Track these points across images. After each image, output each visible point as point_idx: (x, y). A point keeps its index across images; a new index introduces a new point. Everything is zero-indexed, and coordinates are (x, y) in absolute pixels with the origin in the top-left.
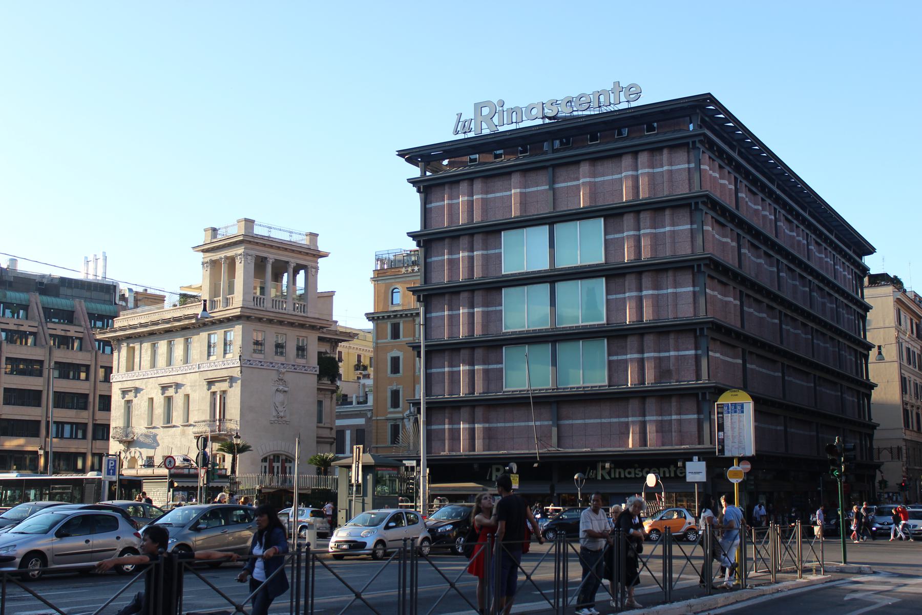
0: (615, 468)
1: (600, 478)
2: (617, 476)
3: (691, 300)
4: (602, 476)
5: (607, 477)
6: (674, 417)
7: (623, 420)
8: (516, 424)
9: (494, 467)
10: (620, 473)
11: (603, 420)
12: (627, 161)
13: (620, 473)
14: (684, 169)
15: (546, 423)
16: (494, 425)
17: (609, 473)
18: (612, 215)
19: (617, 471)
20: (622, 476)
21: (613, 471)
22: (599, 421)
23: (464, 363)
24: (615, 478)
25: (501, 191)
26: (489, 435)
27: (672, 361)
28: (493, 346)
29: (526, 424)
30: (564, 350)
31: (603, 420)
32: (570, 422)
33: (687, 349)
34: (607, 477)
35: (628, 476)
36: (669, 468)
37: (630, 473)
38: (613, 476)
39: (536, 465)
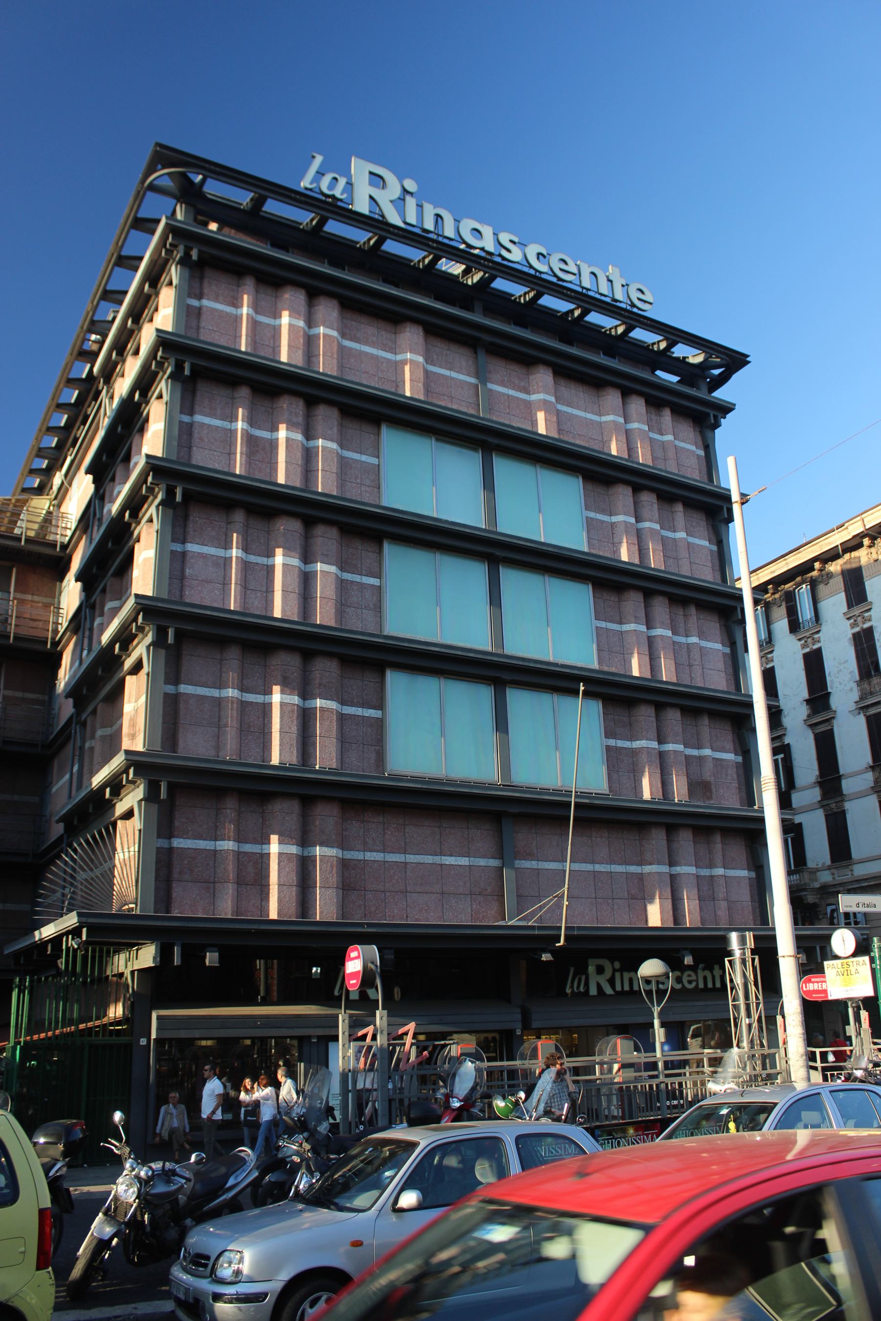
0: (622, 970)
1: (593, 991)
2: (627, 988)
3: (721, 665)
4: (599, 987)
5: (609, 991)
6: (720, 871)
7: (633, 869)
8: (411, 858)
11: (598, 868)
12: (613, 398)
14: (693, 452)
15: (482, 862)
16: (358, 855)
18: (599, 473)
21: (618, 975)
22: (589, 867)
23: (286, 686)
24: (623, 993)
25: (373, 345)
26: (349, 879)
27: (710, 765)
28: (368, 659)
29: (437, 859)
30: (522, 704)
31: (598, 868)
32: (533, 864)
33: (723, 750)
34: (609, 991)
36: (711, 970)
38: (618, 988)
39: (546, 957)
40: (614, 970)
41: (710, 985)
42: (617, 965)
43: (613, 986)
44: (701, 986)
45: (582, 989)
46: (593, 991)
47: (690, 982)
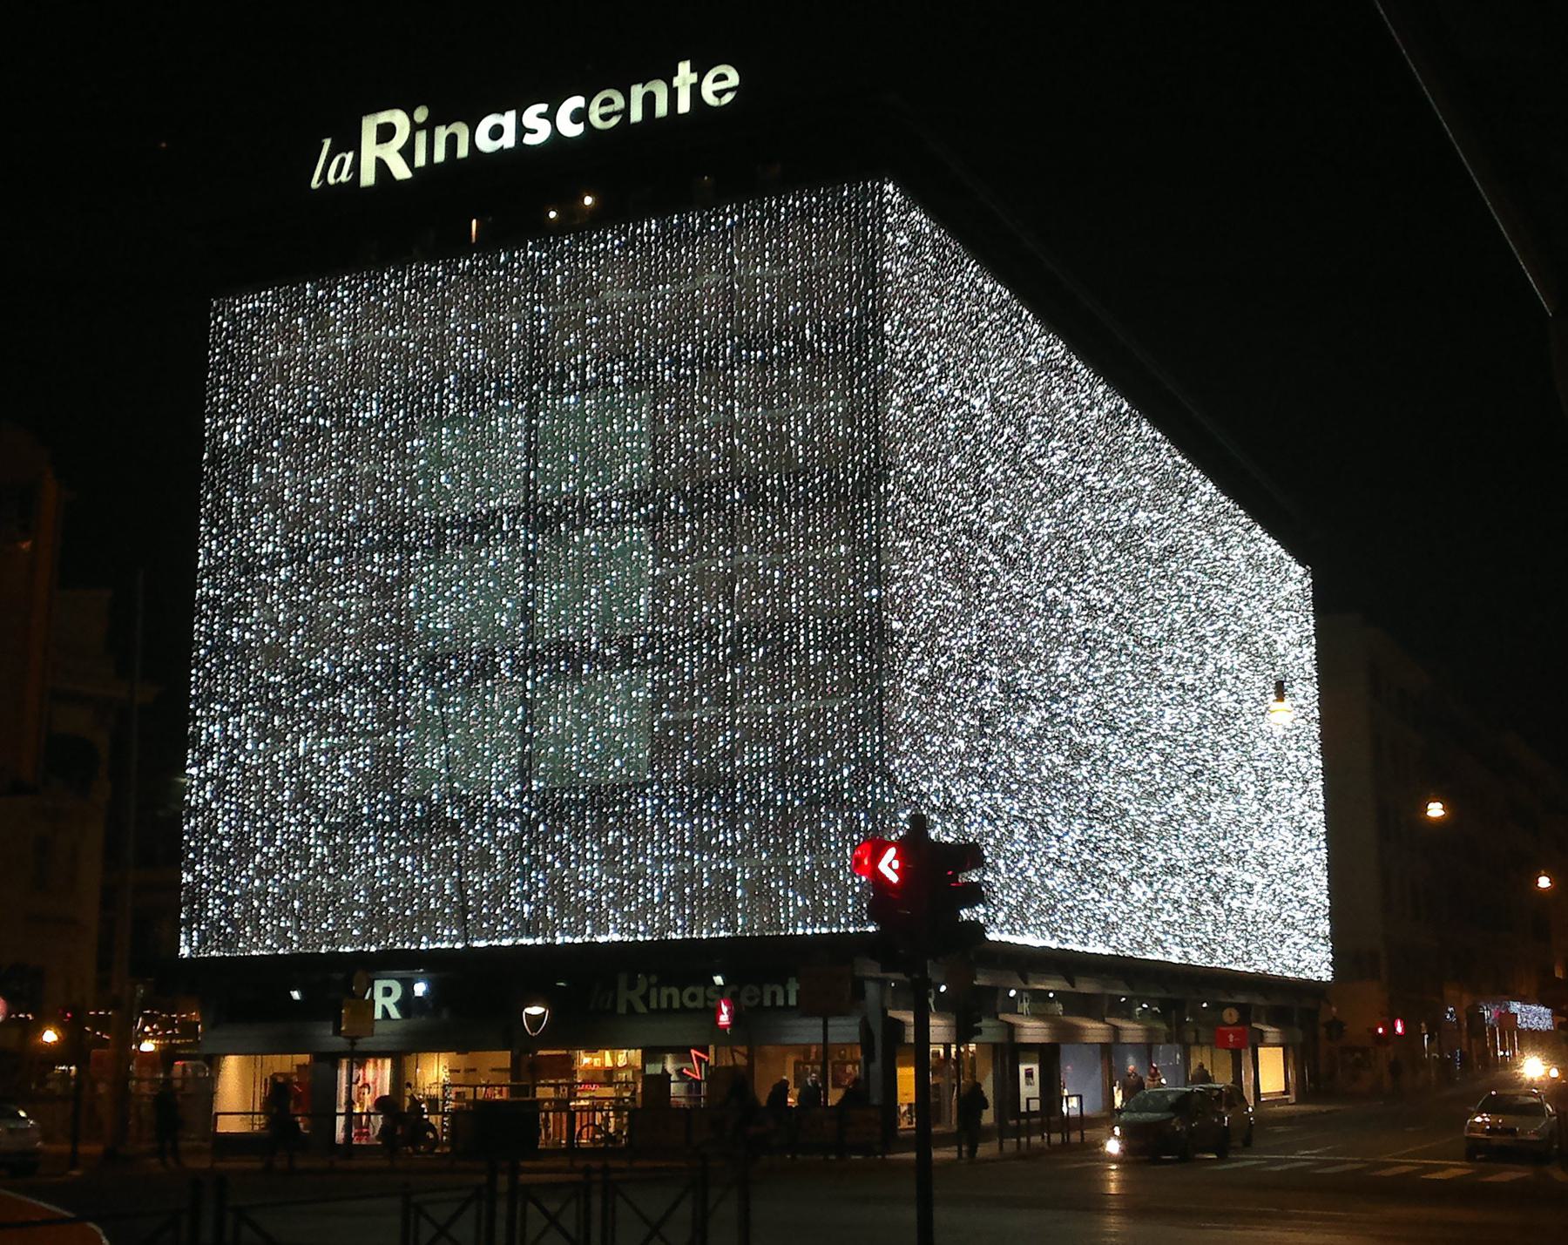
0: (658, 986)
1: (622, 1009)
2: (664, 1005)
5: (641, 1009)
9: (379, 985)
10: (670, 997)
13: (670, 997)
17: (645, 999)
19: (665, 991)
20: (676, 1005)
21: (653, 992)
24: (659, 1011)
34: (641, 1009)
35: (690, 1005)
36: (784, 986)
37: (693, 997)
38: (653, 1005)
40: (650, 986)
41: (780, 1002)
42: (654, 979)
43: (647, 1006)
44: (767, 1003)
45: (608, 1006)
46: (622, 1009)
47: (751, 999)
